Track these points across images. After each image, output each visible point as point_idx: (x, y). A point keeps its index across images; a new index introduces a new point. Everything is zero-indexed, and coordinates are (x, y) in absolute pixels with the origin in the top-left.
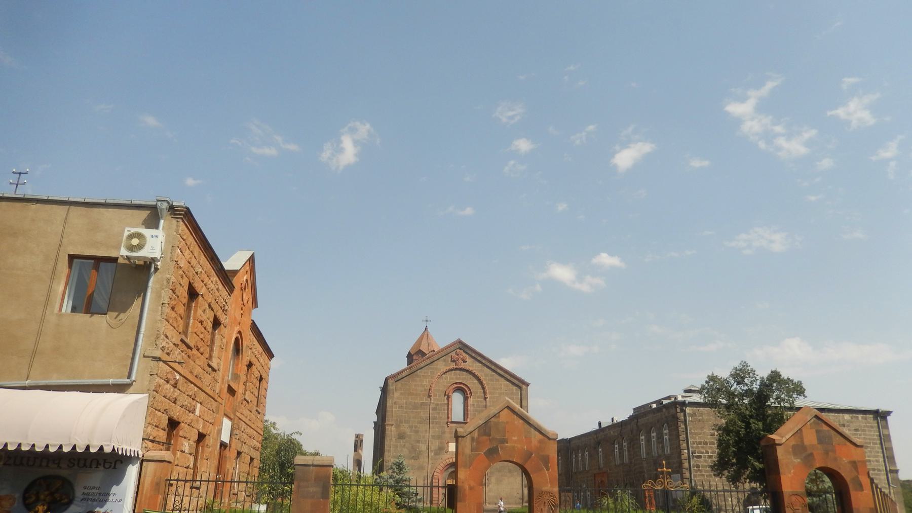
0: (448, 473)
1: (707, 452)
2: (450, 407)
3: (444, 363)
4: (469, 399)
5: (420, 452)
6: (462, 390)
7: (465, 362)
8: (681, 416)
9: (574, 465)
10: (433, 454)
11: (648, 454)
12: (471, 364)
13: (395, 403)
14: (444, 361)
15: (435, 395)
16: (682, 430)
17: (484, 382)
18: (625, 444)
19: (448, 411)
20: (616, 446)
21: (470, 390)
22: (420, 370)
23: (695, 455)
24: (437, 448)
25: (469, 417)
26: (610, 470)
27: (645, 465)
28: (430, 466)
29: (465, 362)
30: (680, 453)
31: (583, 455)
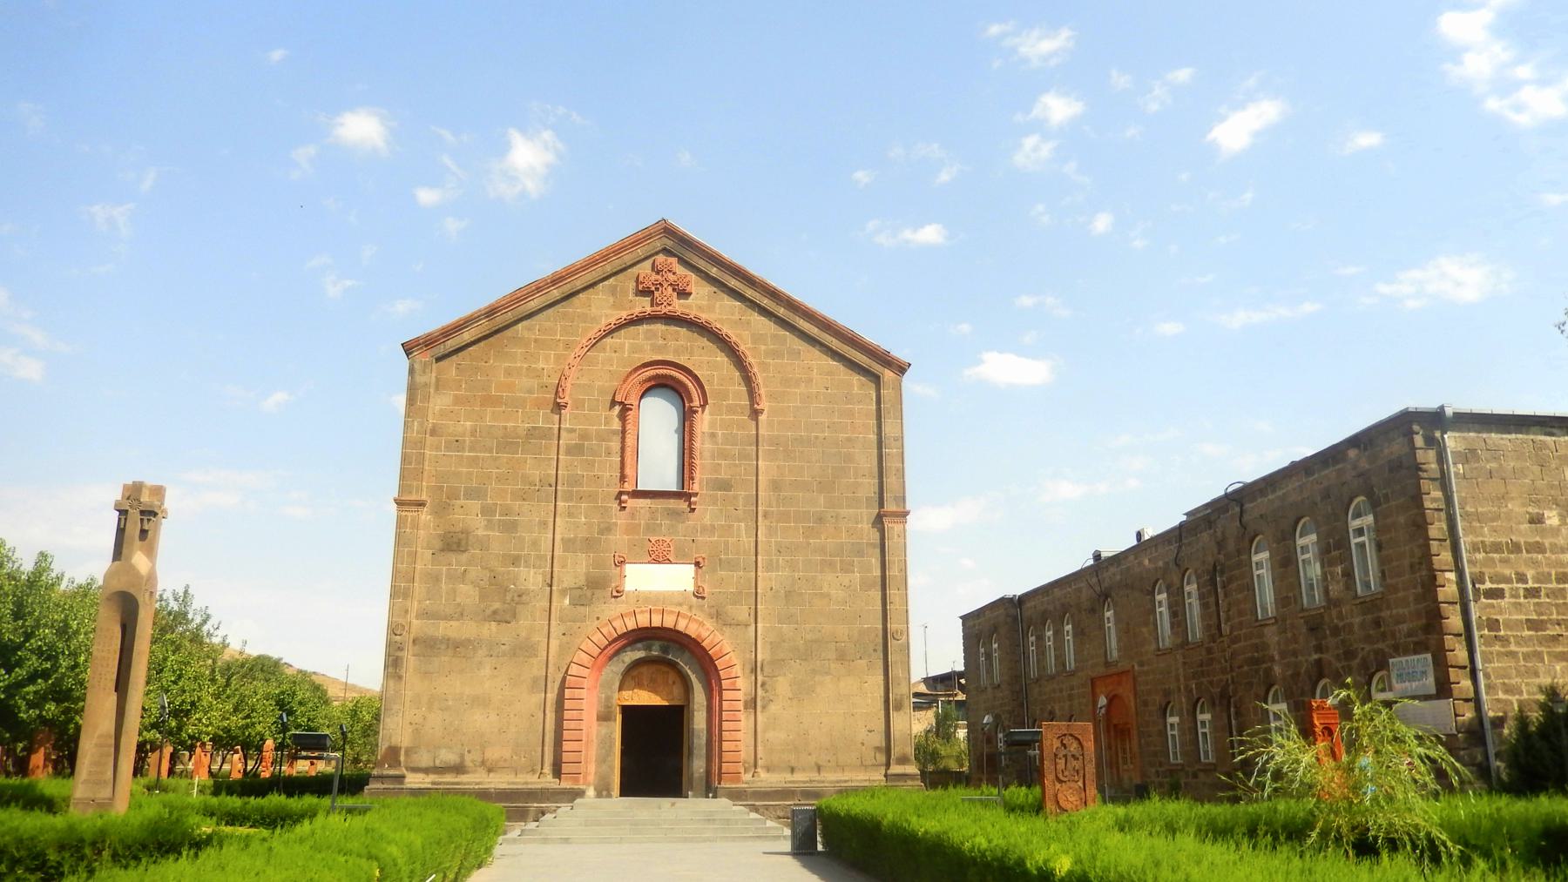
0: (621, 668)
1: (1522, 578)
2: (630, 441)
3: (611, 300)
4: (698, 416)
5: (519, 596)
6: (673, 389)
7: (684, 294)
8: (1427, 457)
9: (1033, 659)
10: (567, 601)
11: (1283, 601)
12: (702, 301)
13: (434, 432)
14: (613, 291)
15: (579, 405)
16: (1435, 505)
17: (750, 359)
18: (1191, 588)
19: (623, 457)
20: (1162, 597)
21: (701, 386)
22: (525, 323)
23: (1482, 587)
24: (582, 581)
25: (697, 475)
26: (1141, 664)
27: (1272, 636)
28: (554, 643)
29: (684, 294)
30: (1431, 583)
31: (1058, 633)
